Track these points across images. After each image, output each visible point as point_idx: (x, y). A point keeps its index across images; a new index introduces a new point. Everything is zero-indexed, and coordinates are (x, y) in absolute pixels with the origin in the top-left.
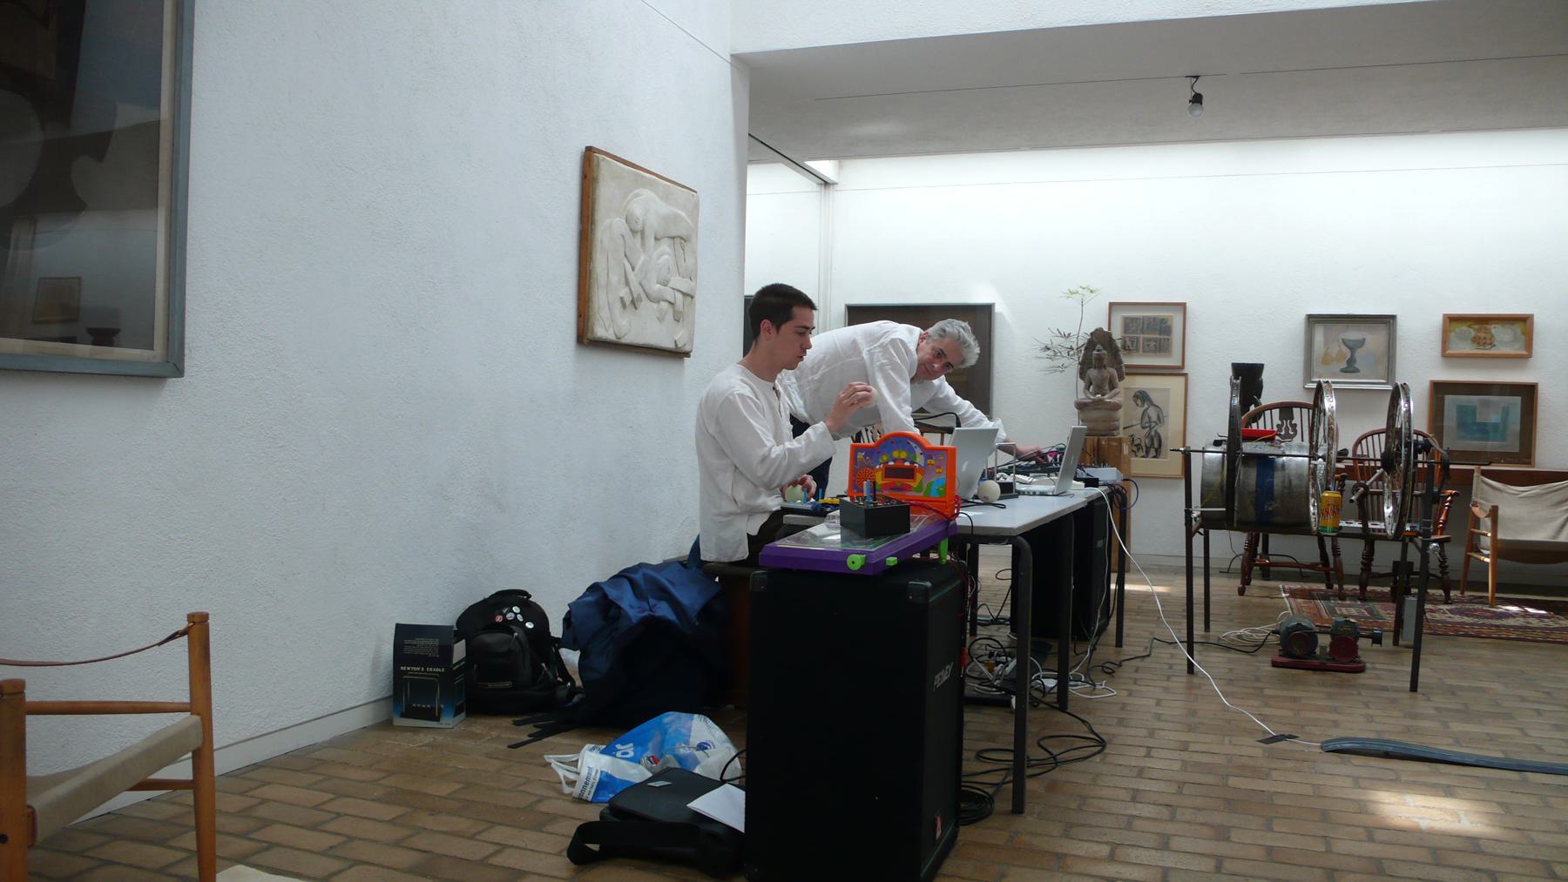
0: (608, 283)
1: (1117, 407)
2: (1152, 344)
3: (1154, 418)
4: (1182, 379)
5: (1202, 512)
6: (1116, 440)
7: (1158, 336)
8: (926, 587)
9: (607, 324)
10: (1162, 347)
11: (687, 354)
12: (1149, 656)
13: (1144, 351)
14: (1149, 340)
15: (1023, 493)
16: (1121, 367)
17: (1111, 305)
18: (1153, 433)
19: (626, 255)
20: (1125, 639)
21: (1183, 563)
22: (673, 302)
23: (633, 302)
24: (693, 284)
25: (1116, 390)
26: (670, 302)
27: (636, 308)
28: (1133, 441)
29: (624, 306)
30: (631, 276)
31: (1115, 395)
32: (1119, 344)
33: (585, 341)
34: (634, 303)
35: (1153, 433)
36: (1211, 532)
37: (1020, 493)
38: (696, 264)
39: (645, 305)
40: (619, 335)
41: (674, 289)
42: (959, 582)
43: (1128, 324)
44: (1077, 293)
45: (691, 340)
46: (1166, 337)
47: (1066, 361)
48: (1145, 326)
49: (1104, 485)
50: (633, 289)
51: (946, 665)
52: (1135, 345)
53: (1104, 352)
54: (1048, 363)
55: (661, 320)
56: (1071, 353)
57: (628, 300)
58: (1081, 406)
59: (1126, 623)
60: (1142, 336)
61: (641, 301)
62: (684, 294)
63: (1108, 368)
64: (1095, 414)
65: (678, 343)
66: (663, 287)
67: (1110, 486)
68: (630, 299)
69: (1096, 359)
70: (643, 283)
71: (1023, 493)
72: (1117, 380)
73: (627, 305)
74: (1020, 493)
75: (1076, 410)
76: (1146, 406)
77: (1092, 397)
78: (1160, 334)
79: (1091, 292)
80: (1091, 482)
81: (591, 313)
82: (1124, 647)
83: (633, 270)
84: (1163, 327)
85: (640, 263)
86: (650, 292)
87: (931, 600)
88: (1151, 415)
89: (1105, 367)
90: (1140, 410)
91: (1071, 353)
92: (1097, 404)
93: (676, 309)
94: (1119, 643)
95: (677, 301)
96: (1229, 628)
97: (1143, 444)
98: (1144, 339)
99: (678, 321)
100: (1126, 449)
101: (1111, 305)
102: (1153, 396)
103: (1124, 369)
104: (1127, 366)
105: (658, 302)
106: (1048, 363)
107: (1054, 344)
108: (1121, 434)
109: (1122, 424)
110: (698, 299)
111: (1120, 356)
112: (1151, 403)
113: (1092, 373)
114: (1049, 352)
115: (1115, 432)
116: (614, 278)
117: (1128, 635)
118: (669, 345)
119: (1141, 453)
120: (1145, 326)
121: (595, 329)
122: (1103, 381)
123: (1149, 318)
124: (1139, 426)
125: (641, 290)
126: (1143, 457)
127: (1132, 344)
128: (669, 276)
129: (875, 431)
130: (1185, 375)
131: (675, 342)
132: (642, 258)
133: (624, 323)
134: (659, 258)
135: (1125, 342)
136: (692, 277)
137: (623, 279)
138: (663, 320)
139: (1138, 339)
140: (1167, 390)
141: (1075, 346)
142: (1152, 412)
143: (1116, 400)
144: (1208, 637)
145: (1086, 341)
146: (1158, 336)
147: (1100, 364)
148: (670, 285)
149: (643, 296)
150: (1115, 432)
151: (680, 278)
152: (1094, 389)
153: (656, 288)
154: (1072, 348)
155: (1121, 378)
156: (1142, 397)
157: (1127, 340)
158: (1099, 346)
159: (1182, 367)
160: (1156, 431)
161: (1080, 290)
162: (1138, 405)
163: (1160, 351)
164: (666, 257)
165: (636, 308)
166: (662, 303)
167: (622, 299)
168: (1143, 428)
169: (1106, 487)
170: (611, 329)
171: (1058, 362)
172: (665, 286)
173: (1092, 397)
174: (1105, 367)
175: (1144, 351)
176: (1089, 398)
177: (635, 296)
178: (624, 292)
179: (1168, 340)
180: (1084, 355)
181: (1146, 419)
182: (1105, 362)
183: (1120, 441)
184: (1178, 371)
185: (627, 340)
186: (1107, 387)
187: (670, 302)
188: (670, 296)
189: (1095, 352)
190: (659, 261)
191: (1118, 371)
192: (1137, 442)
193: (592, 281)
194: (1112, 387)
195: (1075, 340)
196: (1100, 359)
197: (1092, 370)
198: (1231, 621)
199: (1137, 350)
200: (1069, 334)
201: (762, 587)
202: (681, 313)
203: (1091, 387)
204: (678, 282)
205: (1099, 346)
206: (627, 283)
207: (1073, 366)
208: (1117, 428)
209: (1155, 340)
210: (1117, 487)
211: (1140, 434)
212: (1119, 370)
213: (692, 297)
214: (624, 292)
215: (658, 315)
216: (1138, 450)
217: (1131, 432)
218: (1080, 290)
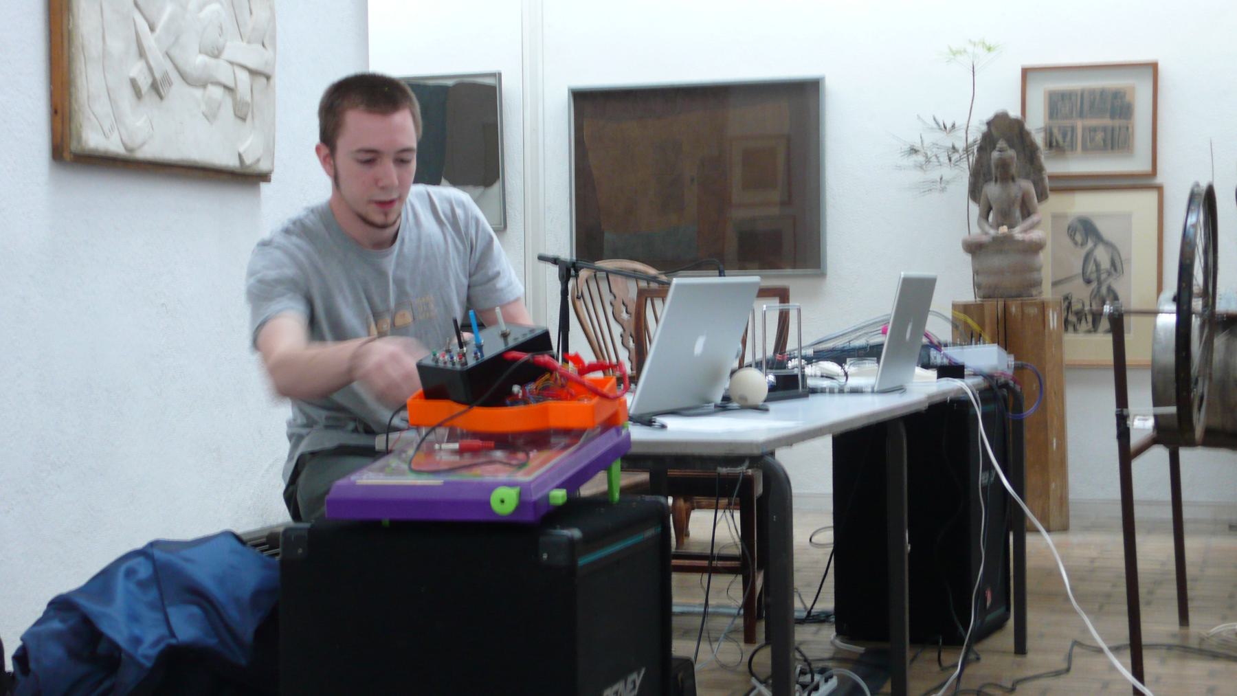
0: (105, 54)
1: (1035, 248)
2: (1099, 137)
3: (1105, 264)
4: (1150, 198)
5: (1156, 417)
6: (1035, 304)
7: (1107, 122)
8: (572, 542)
9: (106, 128)
10: (1117, 141)
11: (265, 177)
12: (1068, 670)
13: (1085, 148)
14: (1094, 130)
15: (822, 391)
16: (1042, 179)
17: (1026, 72)
18: (1104, 290)
19: (136, 5)
20: (1030, 643)
21: (1168, 514)
22: (231, 84)
23: (155, 87)
24: (268, 54)
25: (1034, 218)
26: (226, 88)
27: (161, 97)
28: (1069, 307)
29: (138, 93)
30: (150, 41)
31: (1032, 227)
32: (1039, 139)
33: (66, 155)
34: (156, 88)
35: (1104, 290)
36: (1185, 454)
37: (814, 391)
38: (272, 18)
39: (178, 90)
40: (130, 144)
41: (232, 63)
42: (650, 533)
43: (1056, 103)
44: (965, 51)
45: (270, 151)
46: (1123, 122)
47: (947, 172)
48: (1086, 107)
49: (975, 374)
50: (152, 63)
51: (630, 671)
52: (1068, 138)
53: (1011, 153)
54: (918, 176)
55: (211, 116)
56: (955, 157)
57: (144, 84)
58: (974, 248)
59: (1032, 617)
60: (1079, 124)
61: (170, 84)
62: (253, 73)
63: (1017, 179)
64: (997, 261)
65: (245, 157)
66: (212, 61)
67: (988, 377)
68: (150, 81)
69: (997, 167)
70: (175, 53)
71: (822, 391)
72: (1036, 200)
73: (143, 92)
74: (814, 391)
75: (968, 258)
76: (1090, 244)
77: (992, 232)
78: (1112, 117)
79: (989, 49)
80: (953, 370)
81: (75, 106)
82: (1030, 656)
83: (152, 29)
84: (1119, 106)
85: (165, 17)
86: (188, 69)
87: (582, 561)
88: (1098, 258)
89: (1013, 179)
90: (1083, 252)
91: (955, 157)
92: (1001, 244)
93: (238, 98)
94: (1020, 648)
95: (239, 84)
96: (1224, 619)
97: (1087, 308)
98: (1084, 129)
99: (243, 119)
100: (1053, 320)
101: (1026, 72)
102: (1103, 227)
103: (1047, 181)
104: (1053, 178)
105: (204, 86)
106: (918, 176)
107: (926, 144)
108: (1047, 293)
109: (1047, 275)
110: (277, 80)
111: (1038, 159)
112: (1099, 238)
113: (992, 190)
114: (914, 158)
115: (1034, 292)
116: (116, 45)
117: (1042, 636)
118: (230, 162)
119: (1084, 326)
120: (1086, 107)
121: (84, 136)
122: (1011, 204)
123: (1092, 92)
124: (1080, 281)
125: (169, 66)
126: (1089, 332)
127: (1064, 137)
128: (221, 40)
129: (618, 304)
130: (1159, 189)
131: (240, 156)
132: (168, 10)
133: (138, 124)
134: (201, 8)
135: (1051, 134)
136: (265, 40)
137: (134, 48)
138: (215, 116)
139: (1073, 129)
140: (1128, 217)
141: (960, 145)
142: (1102, 255)
143: (1036, 235)
144: (1185, 637)
145: (979, 136)
146: (1107, 122)
147: (1005, 174)
148: (227, 55)
149: (174, 76)
150: (1034, 292)
151: (244, 44)
152: (996, 217)
153: (197, 61)
154: (954, 149)
155: (1042, 196)
156: (1086, 229)
157: (1055, 131)
158: (1001, 144)
159: (1154, 172)
160: (1110, 289)
161: (970, 48)
162: (1076, 243)
163: (1112, 148)
164: (215, 7)
165: (161, 97)
166: (211, 88)
167: (134, 83)
168: (1088, 282)
169: (979, 380)
170: (116, 134)
171: (934, 174)
172: (217, 57)
173: (992, 232)
174: (1013, 179)
175: (1085, 148)
176: (987, 233)
177: (158, 76)
178: (137, 70)
179: (1127, 128)
180: (979, 161)
181: (1091, 267)
182: (1014, 170)
183: (1043, 307)
184: (1145, 182)
185: (149, 152)
186: (1018, 213)
187: (226, 88)
188: (224, 73)
189: (995, 155)
190: (203, 15)
191: (1035, 184)
192: (1076, 306)
193: (73, 50)
194: (1027, 212)
195: (962, 134)
196: (1004, 165)
197: (993, 184)
198: (1231, 607)
199: (1073, 147)
200: (953, 126)
201: (300, 551)
202: (247, 104)
203: (992, 211)
204: (238, 50)
205: (1001, 144)
206: (142, 54)
207: (961, 178)
208: (1037, 284)
209: (1105, 129)
210: (1002, 380)
211: (1081, 294)
212: (1038, 183)
213: (268, 78)
214: (137, 70)
215: (203, 108)
216: (1080, 320)
217: (1065, 289)
218: (970, 48)
